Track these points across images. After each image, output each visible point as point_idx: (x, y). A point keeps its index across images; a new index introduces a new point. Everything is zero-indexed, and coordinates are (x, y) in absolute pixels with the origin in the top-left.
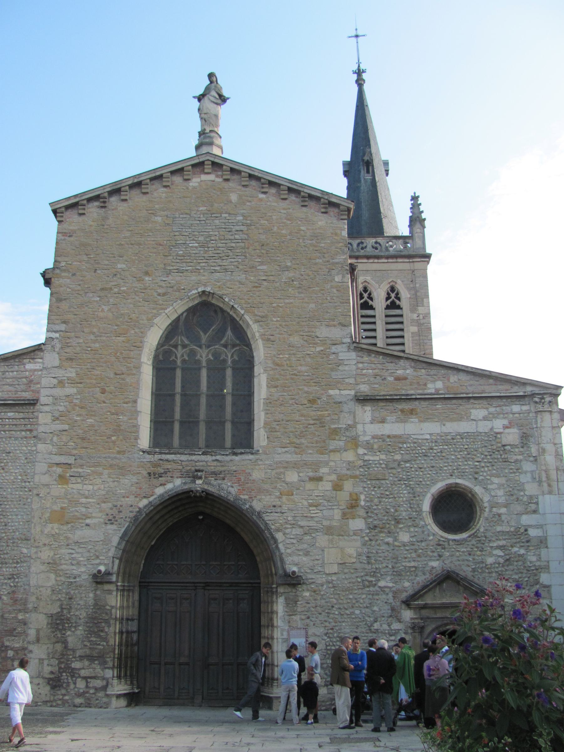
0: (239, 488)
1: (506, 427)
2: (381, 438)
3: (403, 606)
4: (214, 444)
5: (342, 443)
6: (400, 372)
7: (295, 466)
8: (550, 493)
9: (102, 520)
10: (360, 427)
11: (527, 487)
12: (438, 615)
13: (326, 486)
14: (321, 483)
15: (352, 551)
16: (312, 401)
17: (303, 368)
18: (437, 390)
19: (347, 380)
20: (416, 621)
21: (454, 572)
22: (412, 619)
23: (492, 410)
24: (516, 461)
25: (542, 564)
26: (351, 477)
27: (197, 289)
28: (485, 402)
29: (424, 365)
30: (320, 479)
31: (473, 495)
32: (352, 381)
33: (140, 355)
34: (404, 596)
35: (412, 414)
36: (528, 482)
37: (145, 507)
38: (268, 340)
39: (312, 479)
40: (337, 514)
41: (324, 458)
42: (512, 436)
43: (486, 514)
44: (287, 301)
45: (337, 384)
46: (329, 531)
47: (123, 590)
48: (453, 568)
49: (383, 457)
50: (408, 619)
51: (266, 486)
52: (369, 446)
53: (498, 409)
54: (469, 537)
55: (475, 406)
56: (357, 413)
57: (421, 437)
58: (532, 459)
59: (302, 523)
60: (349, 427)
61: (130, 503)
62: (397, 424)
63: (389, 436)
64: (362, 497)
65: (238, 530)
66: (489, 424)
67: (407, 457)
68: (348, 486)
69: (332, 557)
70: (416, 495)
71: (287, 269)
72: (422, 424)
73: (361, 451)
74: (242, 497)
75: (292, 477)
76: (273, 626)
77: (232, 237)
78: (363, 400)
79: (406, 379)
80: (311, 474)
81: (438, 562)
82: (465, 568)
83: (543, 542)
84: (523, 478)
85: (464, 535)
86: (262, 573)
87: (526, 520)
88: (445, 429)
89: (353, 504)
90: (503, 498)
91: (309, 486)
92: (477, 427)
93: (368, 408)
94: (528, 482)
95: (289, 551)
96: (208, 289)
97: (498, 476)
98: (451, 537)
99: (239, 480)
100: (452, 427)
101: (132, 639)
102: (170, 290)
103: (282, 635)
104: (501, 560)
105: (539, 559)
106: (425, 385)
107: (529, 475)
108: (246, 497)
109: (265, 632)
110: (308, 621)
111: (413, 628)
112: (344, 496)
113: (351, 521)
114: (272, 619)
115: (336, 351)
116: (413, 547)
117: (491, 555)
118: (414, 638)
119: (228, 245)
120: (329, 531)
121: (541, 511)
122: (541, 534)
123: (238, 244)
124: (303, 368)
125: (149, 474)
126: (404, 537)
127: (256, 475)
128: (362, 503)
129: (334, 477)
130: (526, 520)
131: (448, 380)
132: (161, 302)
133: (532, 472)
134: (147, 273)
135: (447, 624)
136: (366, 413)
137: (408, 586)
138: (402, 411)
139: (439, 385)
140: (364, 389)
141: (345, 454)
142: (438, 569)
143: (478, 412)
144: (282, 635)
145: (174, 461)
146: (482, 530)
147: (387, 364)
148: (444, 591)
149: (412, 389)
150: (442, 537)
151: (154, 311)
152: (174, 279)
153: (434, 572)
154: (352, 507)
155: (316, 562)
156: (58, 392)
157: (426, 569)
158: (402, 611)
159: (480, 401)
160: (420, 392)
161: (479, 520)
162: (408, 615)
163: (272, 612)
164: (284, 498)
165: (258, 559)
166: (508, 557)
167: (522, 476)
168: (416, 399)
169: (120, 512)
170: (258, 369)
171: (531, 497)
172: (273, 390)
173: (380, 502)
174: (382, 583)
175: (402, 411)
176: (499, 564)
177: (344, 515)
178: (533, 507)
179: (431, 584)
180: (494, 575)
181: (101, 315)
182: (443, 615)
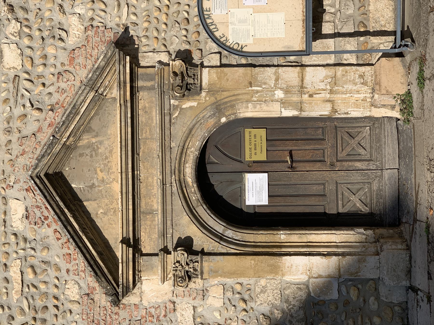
3: (130, 300)
12: (157, 205)
20: (170, 267)
22: (164, 279)
34: (102, 299)
48: (28, 160)
111: (189, 277)
118: (215, 273)
135: (182, 185)
137: (76, 282)
142: (30, 202)
148: (92, 186)
153: (38, 214)
157: (30, 236)
158: (145, 303)
162: (153, 288)
176: (20, 34)
179: (66, 224)
180: (50, 51)
182: (157, 191)
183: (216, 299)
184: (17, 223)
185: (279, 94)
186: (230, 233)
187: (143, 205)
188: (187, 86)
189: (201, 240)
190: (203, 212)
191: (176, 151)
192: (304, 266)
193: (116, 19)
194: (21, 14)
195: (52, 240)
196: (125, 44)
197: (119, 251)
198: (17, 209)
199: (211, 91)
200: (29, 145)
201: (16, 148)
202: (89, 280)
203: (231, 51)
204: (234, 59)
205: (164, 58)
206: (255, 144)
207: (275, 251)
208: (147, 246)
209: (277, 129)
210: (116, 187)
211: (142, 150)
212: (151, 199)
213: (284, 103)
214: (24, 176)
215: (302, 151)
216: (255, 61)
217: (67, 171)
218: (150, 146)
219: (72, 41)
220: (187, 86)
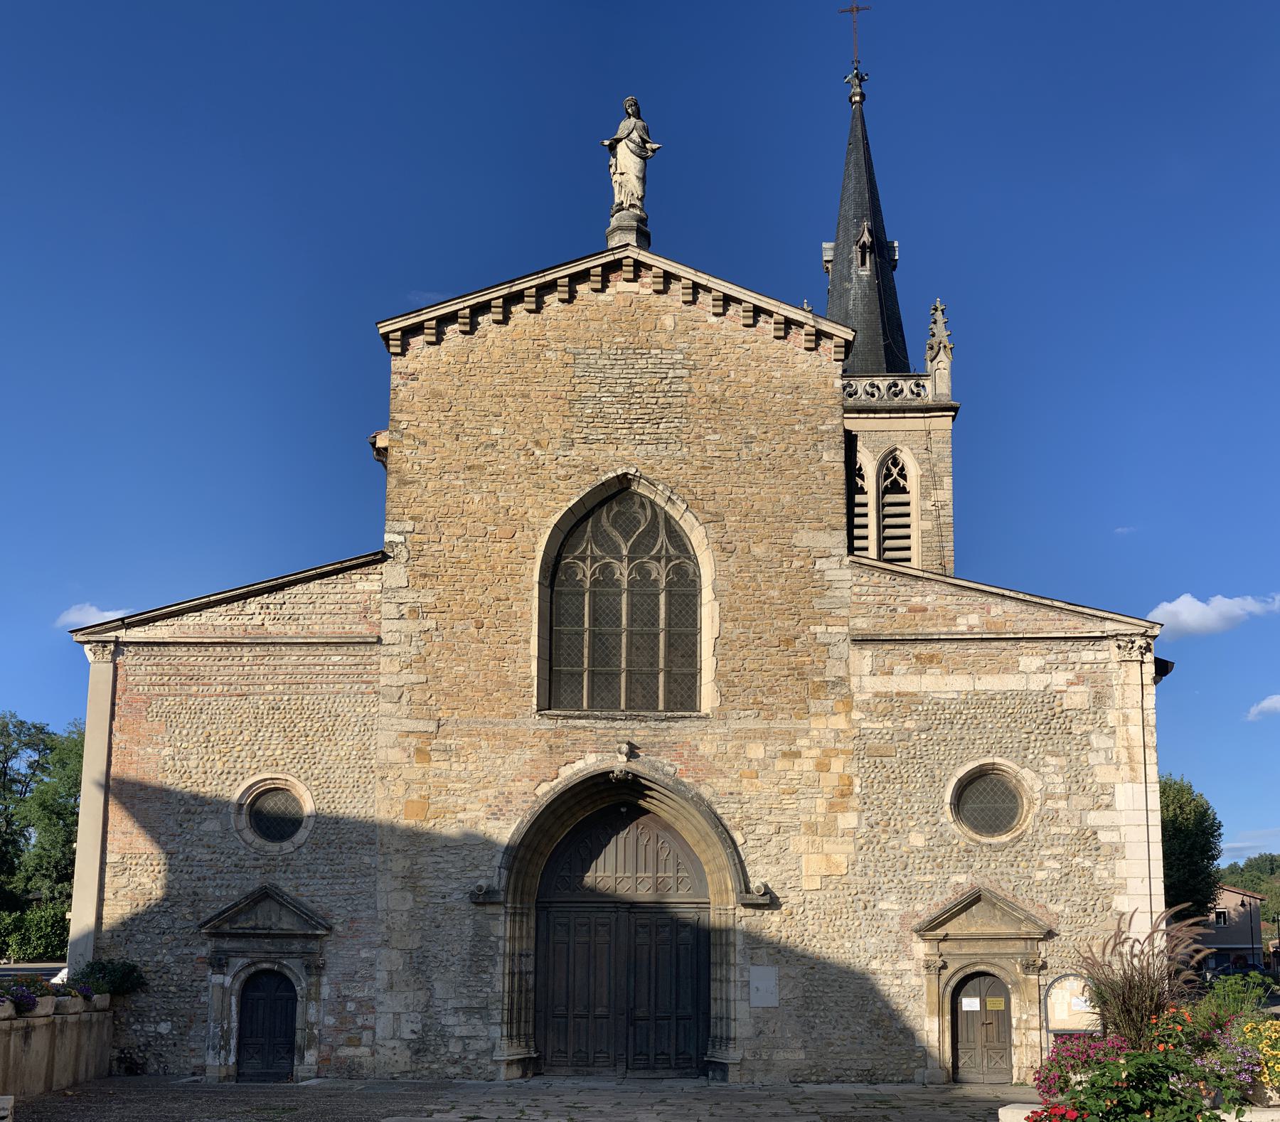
0: (679, 767)
1: (1070, 684)
2: (887, 696)
3: (915, 936)
4: (641, 703)
5: (830, 703)
6: (916, 600)
7: (765, 736)
8: (1133, 781)
9: (481, 814)
10: (854, 681)
11: (1097, 770)
12: (964, 951)
13: (806, 764)
14: (797, 761)
15: (841, 859)
16: (789, 641)
17: (775, 593)
18: (971, 628)
19: (838, 612)
20: (933, 958)
21: (989, 891)
23: (1051, 657)
24: (1086, 734)
25: (1117, 881)
26: (843, 752)
27: (615, 470)
28: (1041, 645)
29: (953, 589)
30: (798, 755)
31: (1019, 781)
32: (844, 612)
33: (532, 570)
34: (915, 923)
35: (931, 662)
36: (1100, 764)
37: (546, 794)
38: (724, 550)
39: (785, 755)
40: (821, 805)
41: (803, 724)
42: (1078, 697)
43: (1036, 809)
44: (749, 490)
45: (822, 617)
46: (812, 828)
47: (514, 914)
48: (987, 884)
49: (889, 724)
50: (922, 956)
51: (718, 764)
52: (867, 708)
53: (1060, 656)
54: (1011, 841)
55: (1025, 651)
56: (852, 659)
57: (943, 696)
58: (1106, 731)
59: (771, 818)
60: (842, 681)
61: (521, 789)
62: (910, 677)
63: (898, 694)
64: (857, 781)
65: (678, 826)
66: (1044, 679)
67: (924, 725)
68: (837, 765)
69: (812, 866)
70: (937, 779)
71: (750, 440)
72: (947, 677)
73: (856, 715)
74: (685, 780)
75: (756, 751)
76: (728, 964)
77: (667, 388)
78: (861, 641)
79: (925, 610)
80: (785, 748)
81: (964, 876)
82: (1004, 886)
83: (1117, 850)
84: (1093, 758)
85: (1005, 838)
86: (711, 890)
87: (1093, 818)
88: (980, 686)
89: (845, 794)
90: (1063, 786)
91: (780, 764)
92: (1027, 683)
93: (868, 653)
94: (1100, 764)
95: (752, 857)
96: (632, 471)
97: (1054, 754)
98: (985, 840)
99: (681, 755)
100: (991, 683)
101: (527, 982)
102: (571, 471)
103: (742, 976)
104: (1057, 876)
105: (1113, 875)
106: (954, 619)
107: (1102, 754)
108: (691, 780)
109: (716, 973)
110: (778, 956)
112: (830, 781)
113: (840, 816)
114: (727, 954)
115: (825, 567)
116: (932, 854)
117: (1041, 867)
118: (929, 981)
119: (661, 401)
120: (812, 828)
121: (1118, 806)
122: (1116, 839)
123: (675, 400)
124: (775, 593)
125: (551, 747)
126: (917, 840)
127: (706, 749)
128: (857, 790)
129: (816, 752)
130: (1093, 818)
131: (989, 612)
132: (561, 489)
133: (1106, 750)
134: (537, 443)
135: (975, 964)
136: (864, 659)
137: (924, 909)
138: (917, 657)
139: (974, 619)
140: (862, 624)
141: (834, 718)
143: (1030, 660)
144: (742, 976)
145: (584, 728)
146: (1030, 832)
147: (898, 588)
149: (935, 625)
150: (971, 840)
151: (553, 504)
152: (578, 453)
154: (843, 795)
155: (791, 873)
156: (411, 626)
159: (1035, 645)
160: (945, 629)
161: (1026, 816)
162: (921, 949)
163: (728, 944)
164: (745, 781)
165: (706, 869)
166: (1066, 871)
167: (1091, 755)
168: (939, 640)
169: (508, 802)
170: (707, 594)
171: (1103, 785)
172: (729, 625)
173: (884, 788)
174: (882, 905)
175: (917, 657)
177: (831, 807)
178: (1106, 799)
179: (956, 906)
180: (1045, 895)
181: (473, 508)
183: (915, 981)
184: (955, 878)
185: (1025, 1017)
186: (949, 989)
187: (964, 943)
188: (1027, 968)
189: (946, 974)
190: (960, 975)
191: (993, 961)
192: (931, 1030)
193: (1063, 929)
194: (1064, 879)
195: (945, 896)
196: (1050, 935)
197: (940, 932)
198: (961, 878)
199: (1025, 980)
200: (995, 885)
201: (993, 878)
202: (925, 917)
203: (1048, 991)
204: (1043, 992)
205: (1043, 955)
206: (996, 1004)
207: (940, 1014)
208: (943, 945)
209: (1005, 1016)
210: (973, 930)
211: (993, 943)
212: (966, 949)
213: (1019, 1020)
214: (979, 882)
215: (993, 1030)
216: (1043, 1004)
217: (981, 904)
218: (996, 948)
219: (1051, 906)
220: (1027, 968)
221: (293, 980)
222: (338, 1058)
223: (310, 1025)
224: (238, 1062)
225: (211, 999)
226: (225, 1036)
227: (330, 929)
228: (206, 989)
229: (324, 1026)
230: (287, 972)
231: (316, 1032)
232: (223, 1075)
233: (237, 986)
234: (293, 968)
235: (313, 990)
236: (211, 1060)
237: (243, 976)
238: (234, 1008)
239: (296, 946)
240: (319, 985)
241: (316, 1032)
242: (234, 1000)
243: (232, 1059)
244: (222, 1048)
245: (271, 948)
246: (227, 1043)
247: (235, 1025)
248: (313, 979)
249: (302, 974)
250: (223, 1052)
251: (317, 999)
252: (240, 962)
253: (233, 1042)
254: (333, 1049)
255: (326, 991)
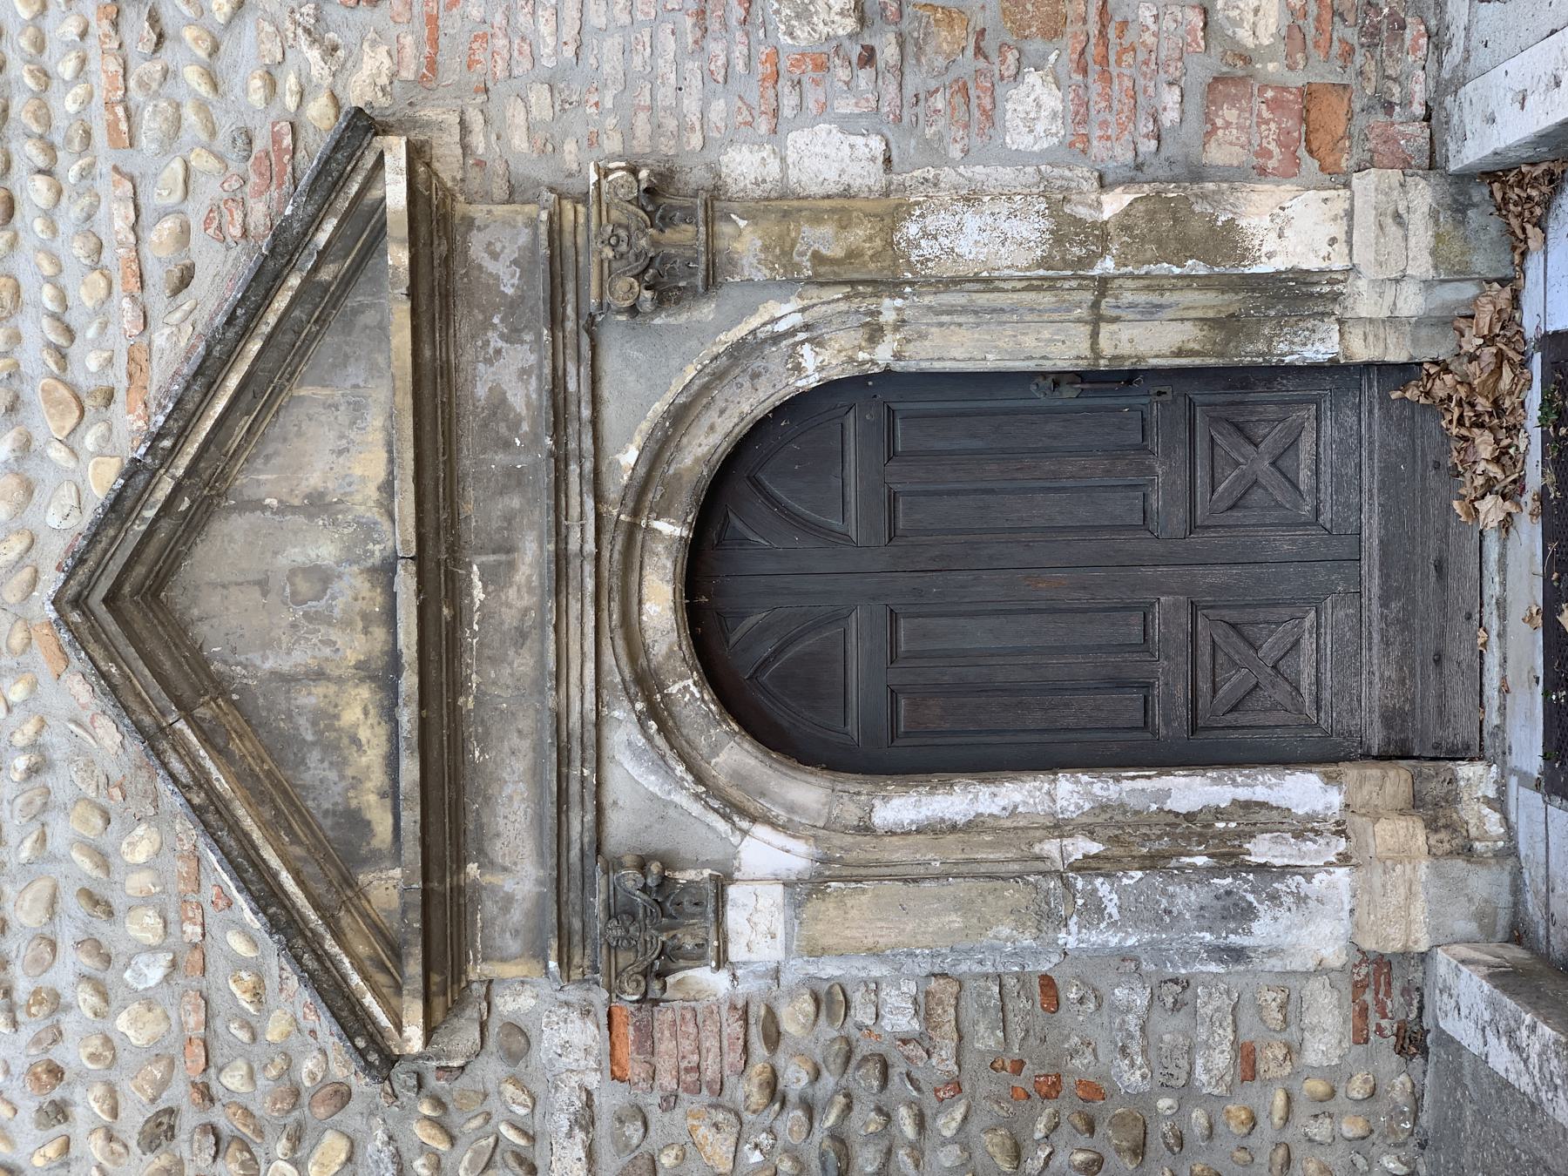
221: (744, 404)
222: (1293, 35)
223: (1072, 239)
224: (1324, 753)
225: (890, 956)
226: (1154, 846)
227: (361, 127)
228: (829, 1001)
229: (1078, 146)
230: (703, 445)
231: (1114, 204)
232: (1412, 832)
233: (807, 792)
234: (664, 393)
235: (821, 238)
236: (1312, 931)
237: (734, 755)
238: (958, 801)
239: (505, 373)
240: (783, 206)
241: (1114, 204)
242: (901, 807)
243: (1302, 791)
244: (1230, 860)
245: (531, 554)
246: (1192, 827)
247: (1070, 792)
248: (745, 242)
249: (709, 326)
250: (1261, 850)
251: (891, 211)
252: (638, 785)
253: (1190, 791)
254: (1232, 78)
255: (828, 154)
